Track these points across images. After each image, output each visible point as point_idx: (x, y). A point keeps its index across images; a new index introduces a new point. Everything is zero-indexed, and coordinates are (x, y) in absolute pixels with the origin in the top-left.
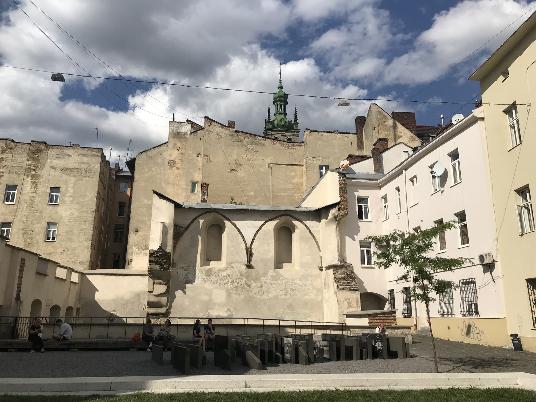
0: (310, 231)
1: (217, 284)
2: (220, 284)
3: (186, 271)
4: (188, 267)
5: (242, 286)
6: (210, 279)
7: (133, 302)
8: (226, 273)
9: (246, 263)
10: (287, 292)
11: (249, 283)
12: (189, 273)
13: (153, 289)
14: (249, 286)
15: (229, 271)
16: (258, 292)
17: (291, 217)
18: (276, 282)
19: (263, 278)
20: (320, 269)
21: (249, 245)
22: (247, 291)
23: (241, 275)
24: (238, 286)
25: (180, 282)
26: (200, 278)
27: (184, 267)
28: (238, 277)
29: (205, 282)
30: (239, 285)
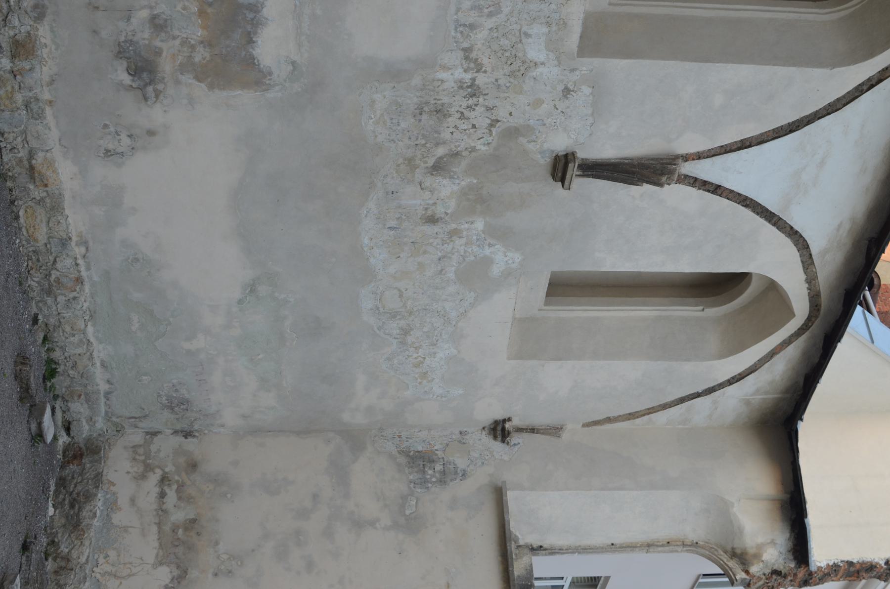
0: (698, 395)
1: (472, 8)
2: (472, 27)
5: (446, 135)
8: (542, 58)
9: (582, 154)
10: (394, 315)
11: (459, 168)
14: (438, 168)
15: (549, 72)
16: (400, 207)
17: (792, 336)
18: (451, 276)
19: (479, 225)
20: (496, 423)
21: (687, 168)
22: (410, 162)
23: (513, 133)
24: (447, 115)
28: (501, 113)
30: (452, 121)
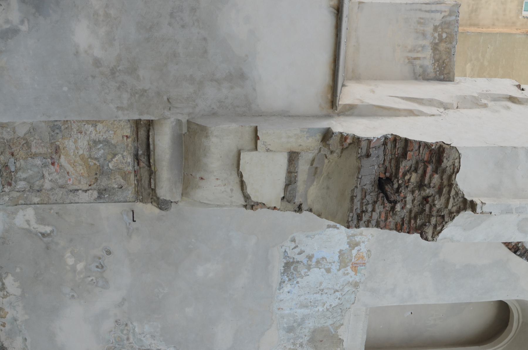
3: (336, 258)
4: (355, 268)
6: (301, 345)
7: (206, 52)
12: (328, 271)
13: (268, 150)
25: (293, 240)
26: (306, 311)
27: (354, 252)
29: (290, 329)
